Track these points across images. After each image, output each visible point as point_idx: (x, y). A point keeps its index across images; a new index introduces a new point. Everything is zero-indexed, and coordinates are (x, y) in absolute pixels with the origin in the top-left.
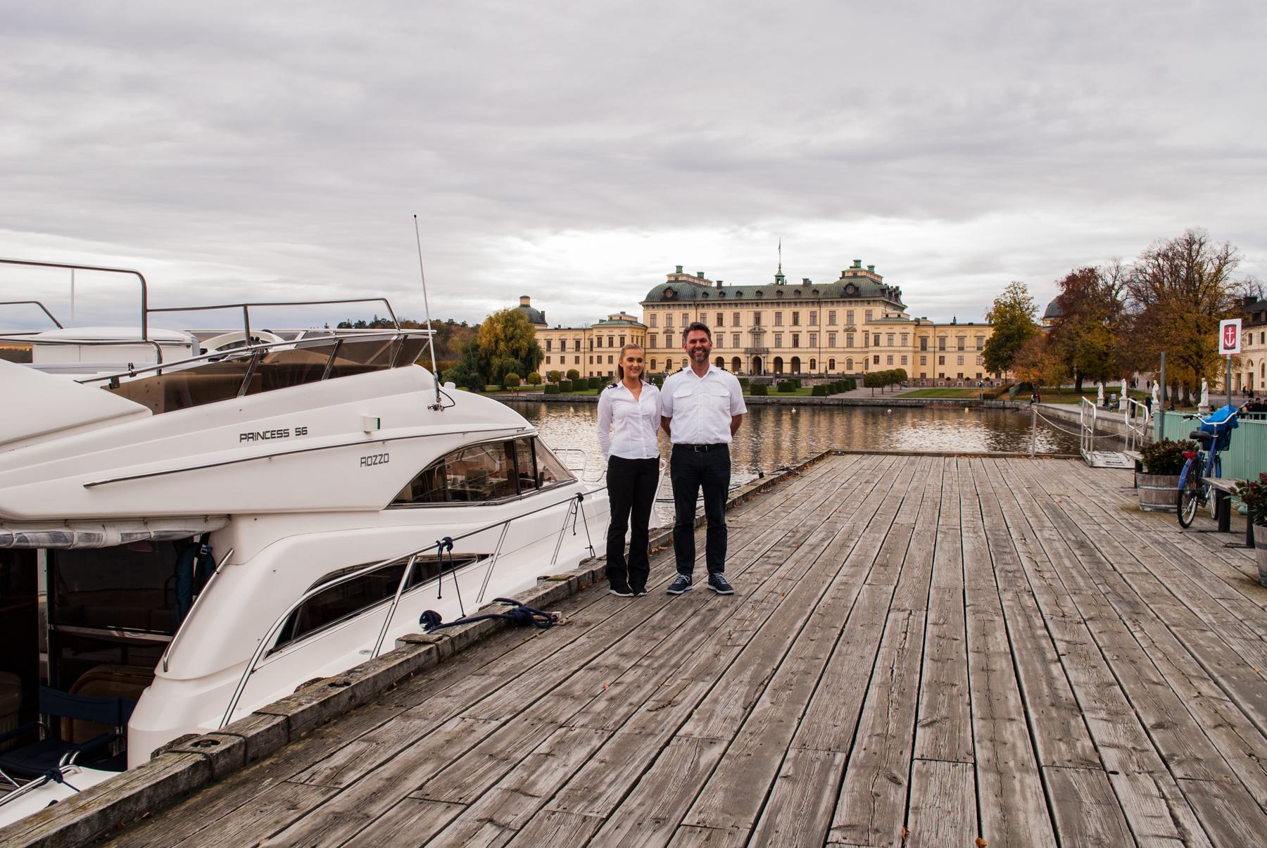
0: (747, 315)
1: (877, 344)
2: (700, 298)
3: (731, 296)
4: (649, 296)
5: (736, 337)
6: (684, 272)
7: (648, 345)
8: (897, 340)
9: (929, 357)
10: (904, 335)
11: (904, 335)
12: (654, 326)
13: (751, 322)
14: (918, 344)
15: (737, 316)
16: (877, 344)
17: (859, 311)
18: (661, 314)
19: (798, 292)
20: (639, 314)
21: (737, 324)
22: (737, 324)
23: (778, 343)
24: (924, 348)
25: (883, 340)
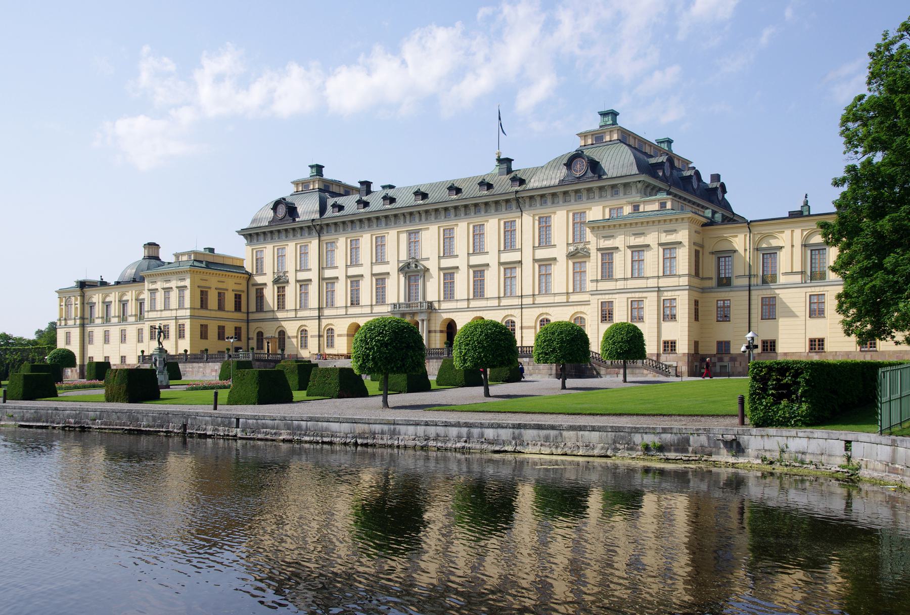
0: (395, 241)
1: (607, 273)
2: (330, 212)
3: (376, 203)
4: (254, 221)
5: (380, 280)
6: (327, 174)
7: (253, 307)
8: (652, 261)
9: (737, 300)
10: (669, 248)
11: (669, 248)
12: (260, 271)
13: (404, 257)
14: (709, 267)
15: (380, 245)
16: (607, 273)
17: (596, 212)
18: (269, 250)
19: (486, 185)
20: (237, 249)
21: (379, 259)
22: (379, 259)
23: (449, 293)
24: (724, 282)
25: (621, 263)
